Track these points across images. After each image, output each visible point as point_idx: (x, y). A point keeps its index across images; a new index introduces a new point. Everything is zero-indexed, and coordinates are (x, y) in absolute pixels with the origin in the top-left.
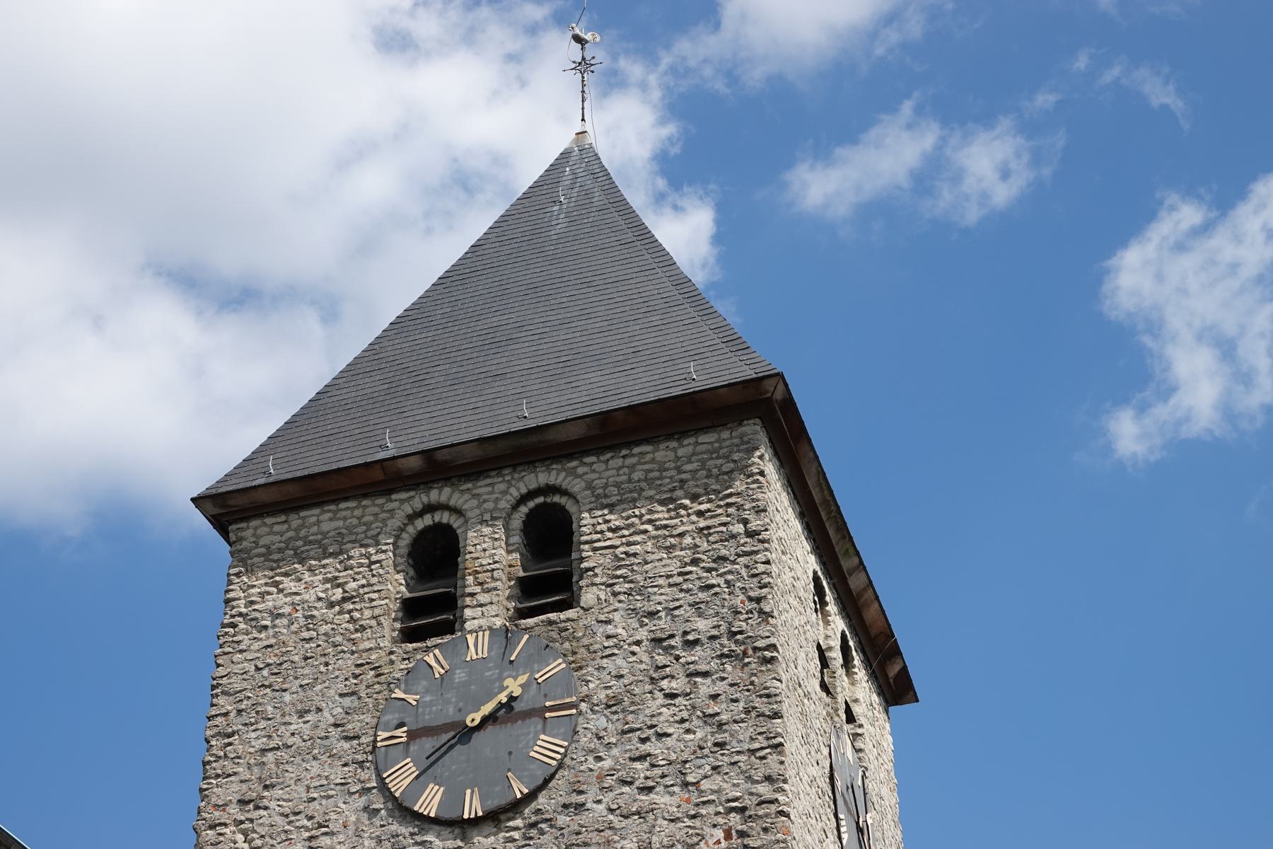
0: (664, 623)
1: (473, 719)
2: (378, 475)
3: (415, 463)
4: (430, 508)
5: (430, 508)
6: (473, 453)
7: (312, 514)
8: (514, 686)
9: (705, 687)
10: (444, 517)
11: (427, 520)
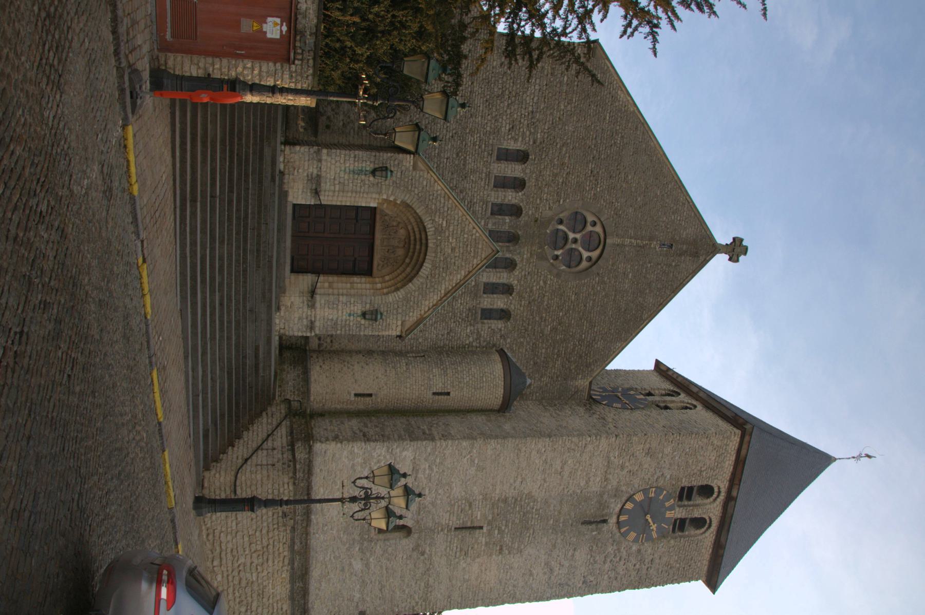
0: (657, 561)
1: (648, 517)
2: (736, 482)
3: (734, 493)
4: (719, 492)
5: (719, 492)
6: (729, 510)
7: (733, 458)
8: (654, 527)
9: (634, 573)
10: (715, 496)
11: (716, 490)
